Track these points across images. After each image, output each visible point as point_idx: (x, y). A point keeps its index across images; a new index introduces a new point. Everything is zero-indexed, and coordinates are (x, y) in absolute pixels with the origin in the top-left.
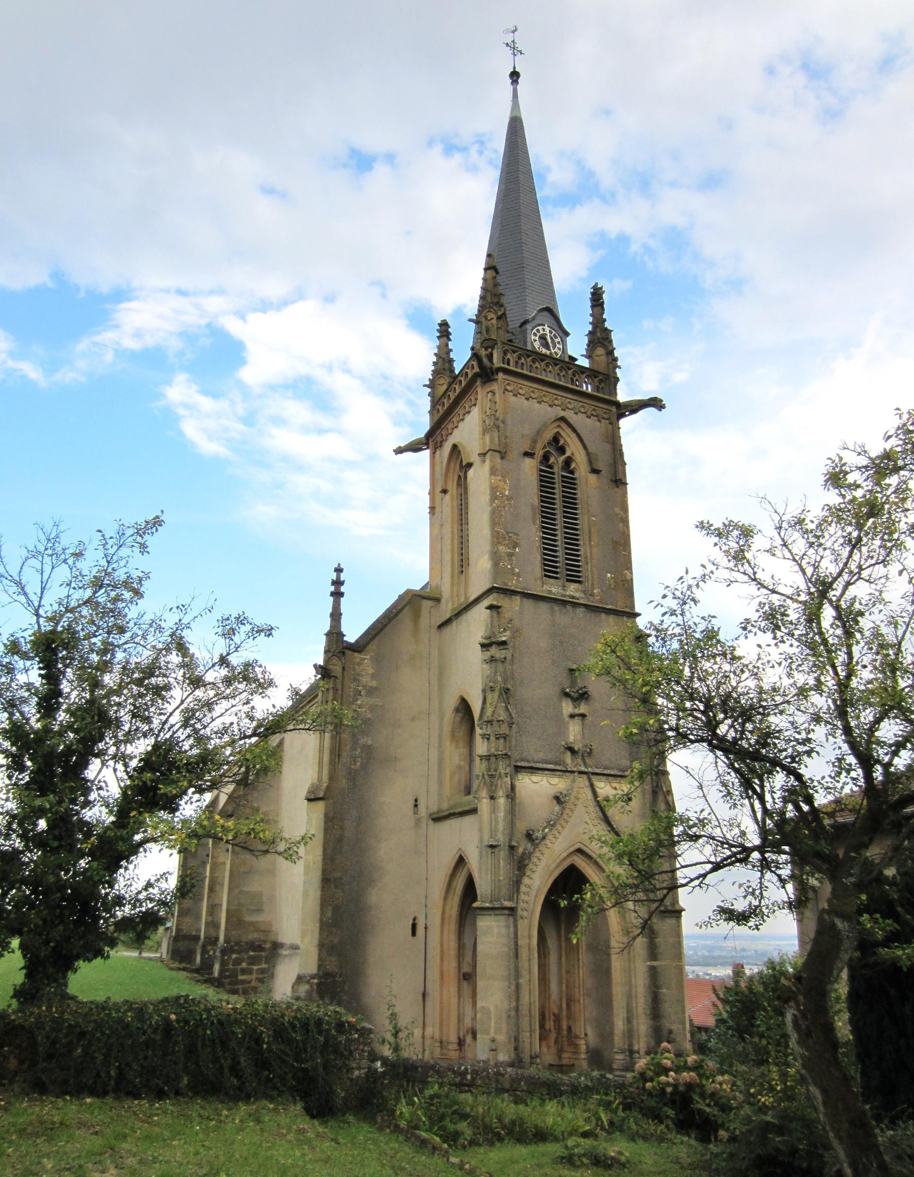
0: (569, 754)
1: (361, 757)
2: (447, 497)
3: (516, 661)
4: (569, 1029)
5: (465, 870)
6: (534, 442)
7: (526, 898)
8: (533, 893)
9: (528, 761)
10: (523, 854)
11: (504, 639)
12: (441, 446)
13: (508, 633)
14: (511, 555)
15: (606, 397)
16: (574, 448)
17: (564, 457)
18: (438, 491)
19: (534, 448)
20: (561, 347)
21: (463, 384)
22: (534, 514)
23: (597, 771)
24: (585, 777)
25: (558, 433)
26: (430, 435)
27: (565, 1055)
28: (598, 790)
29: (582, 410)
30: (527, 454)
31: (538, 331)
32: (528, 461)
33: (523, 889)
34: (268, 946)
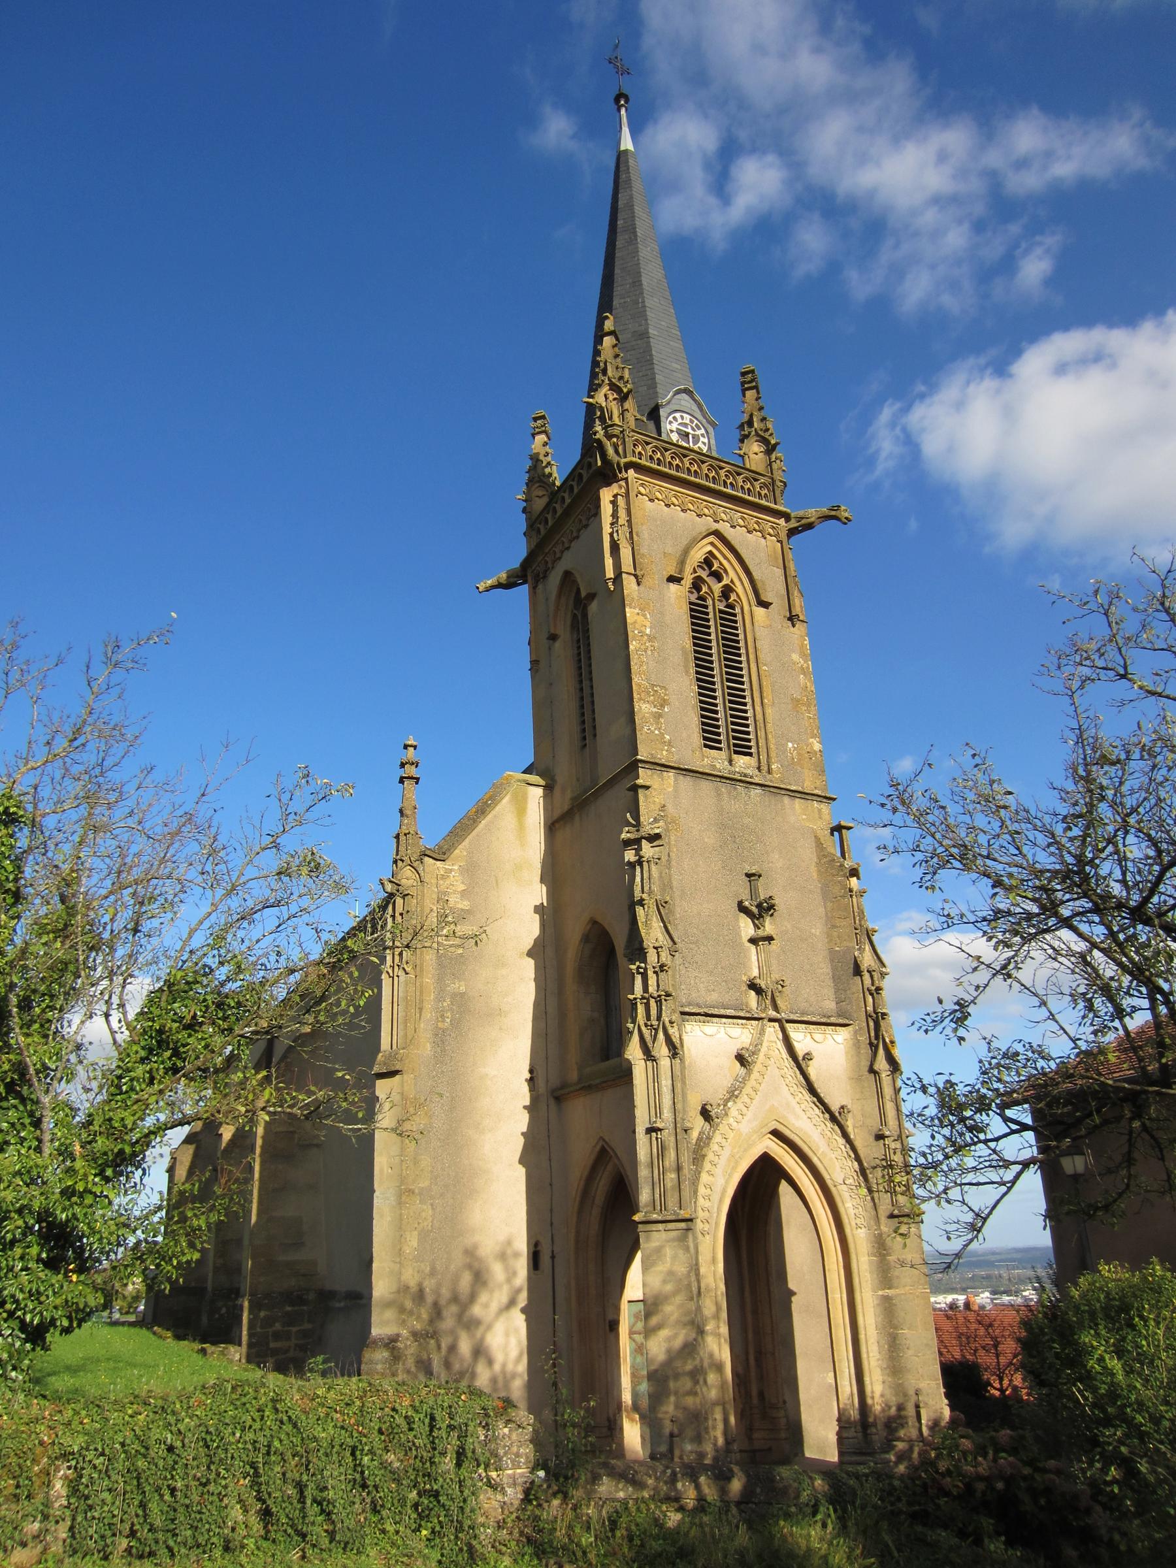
0: (753, 993)
1: (452, 1010)
2: (557, 644)
3: (673, 863)
4: (761, 1395)
5: (610, 1167)
6: (682, 563)
7: (707, 1204)
8: (716, 1198)
9: (699, 1006)
10: (699, 1139)
11: (657, 831)
12: (545, 577)
13: (661, 823)
14: (658, 716)
15: (772, 505)
16: (734, 574)
17: (721, 584)
18: (542, 640)
19: (681, 571)
20: (706, 440)
21: (576, 490)
22: (686, 660)
23: (793, 1017)
24: (776, 1025)
25: (710, 552)
26: (526, 564)
27: (756, 1435)
28: (795, 1044)
29: (741, 523)
30: (672, 579)
31: (675, 418)
32: (673, 587)
33: (702, 1190)
34: (311, 1296)
